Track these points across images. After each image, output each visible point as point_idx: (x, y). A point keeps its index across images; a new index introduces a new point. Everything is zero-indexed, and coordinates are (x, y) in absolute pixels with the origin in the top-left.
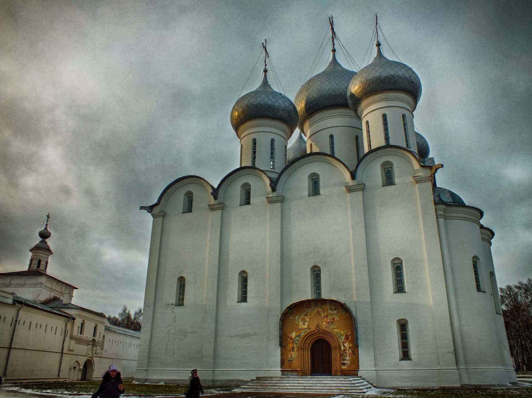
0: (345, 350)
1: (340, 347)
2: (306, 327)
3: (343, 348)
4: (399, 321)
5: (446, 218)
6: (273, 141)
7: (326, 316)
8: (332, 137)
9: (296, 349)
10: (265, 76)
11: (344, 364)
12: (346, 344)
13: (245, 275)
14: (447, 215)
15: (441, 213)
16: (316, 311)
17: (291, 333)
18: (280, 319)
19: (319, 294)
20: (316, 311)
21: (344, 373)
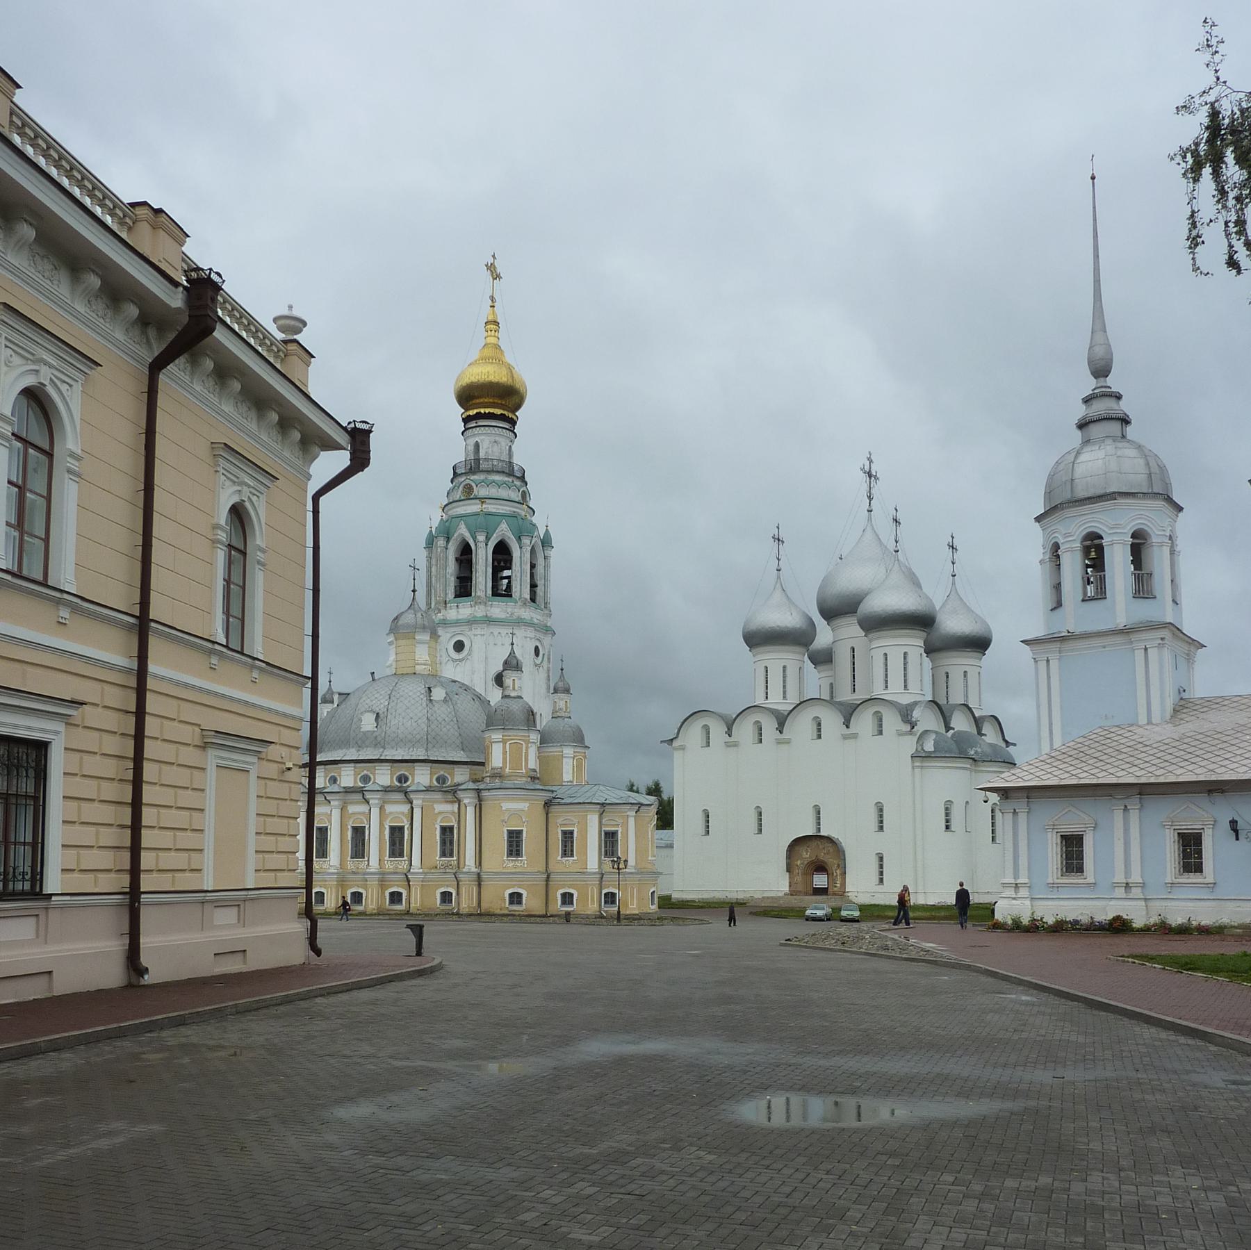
0: (837, 876)
1: (833, 873)
2: (808, 856)
3: (835, 874)
4: (877, 854)
5: (922, 767)
6: (784, 667)
7: (824, 848)
8: (853, 650)
9: (800, 875)
11: (836, 887)
12: (838, 871)
13: (759, 809)
15: (918, 764)
16: (816, 844)
17: (797, 860)
18: (787, 851)
19: (819, 830)
20: (816, 844)
21: (835, 894)
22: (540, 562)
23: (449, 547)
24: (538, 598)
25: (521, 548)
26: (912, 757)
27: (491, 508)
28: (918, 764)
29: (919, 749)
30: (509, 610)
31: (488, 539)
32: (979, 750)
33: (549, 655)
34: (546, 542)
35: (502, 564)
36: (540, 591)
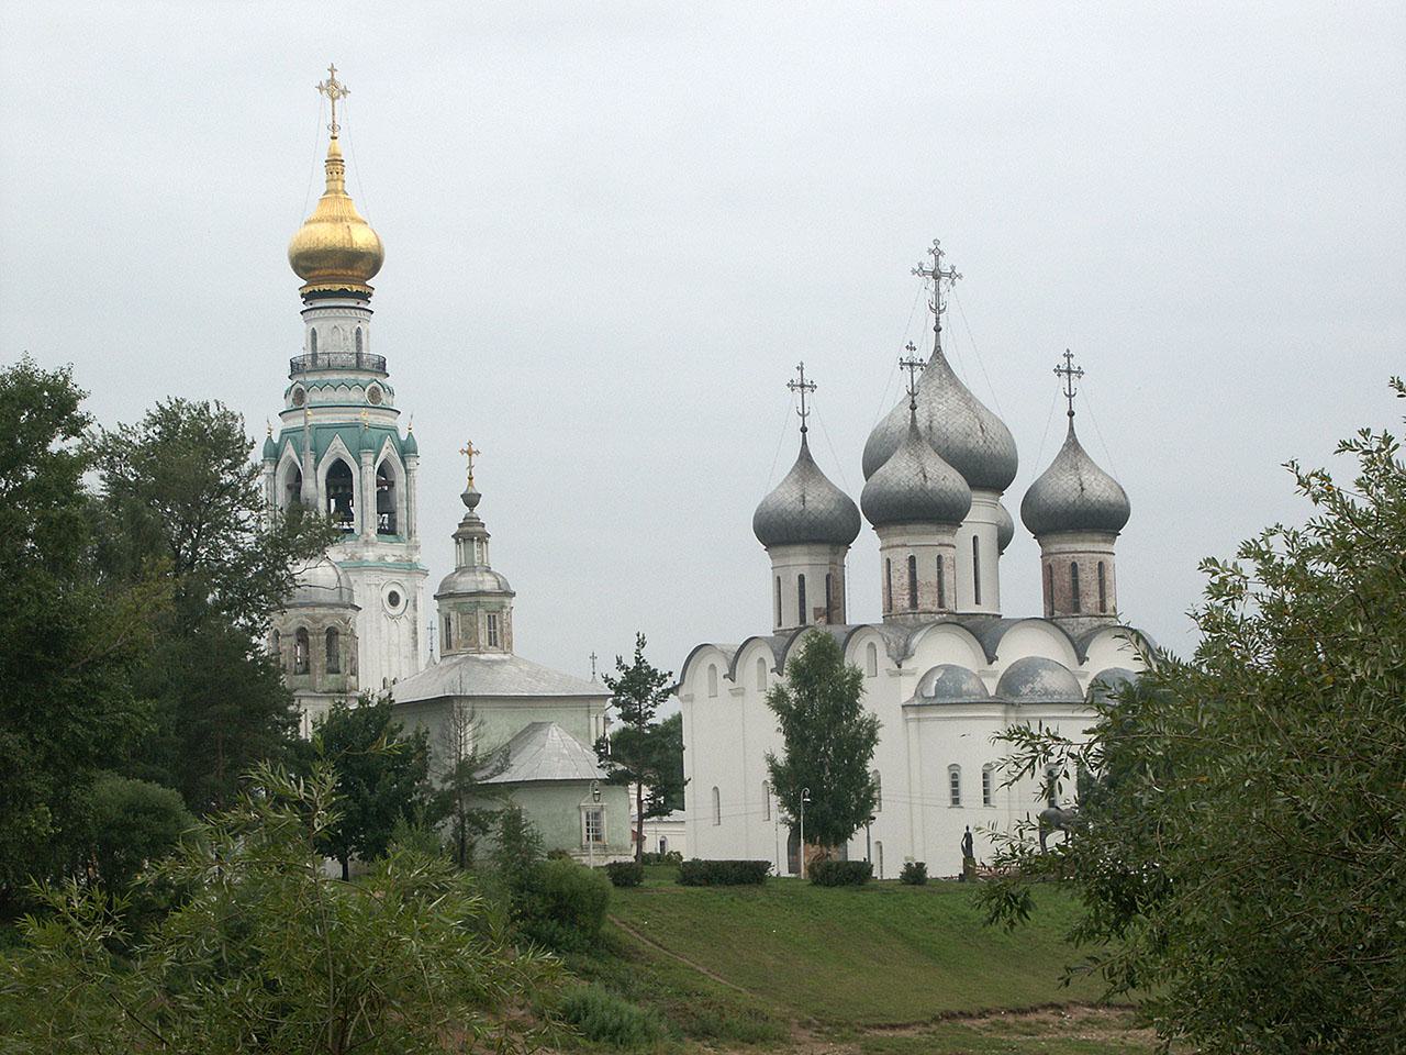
5: (919, 719)
10: (804, 442)
14: (921, 716)
15: (910, 716)
22: (400, 478)
23: (277, 472)
24: (398, 528)
25: (361, 468)
26: (903, 706)
27: (326, 418)
28: (910, 716)
29: (919, 693)
30: (349, 550)
31: (317, 461)
32: (1038, 686)
33: (415, 601)
34: (407, 450)
35: (340, 491)
36: (401, 518)
